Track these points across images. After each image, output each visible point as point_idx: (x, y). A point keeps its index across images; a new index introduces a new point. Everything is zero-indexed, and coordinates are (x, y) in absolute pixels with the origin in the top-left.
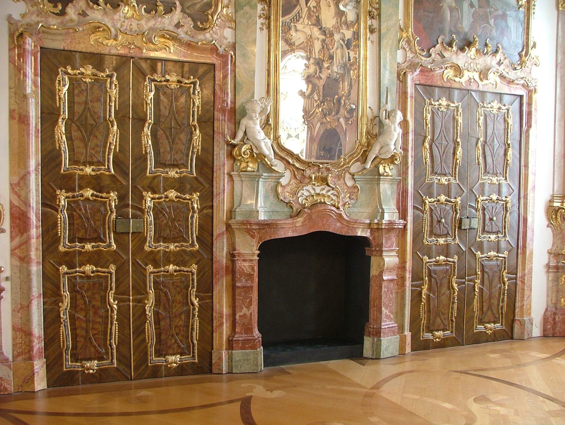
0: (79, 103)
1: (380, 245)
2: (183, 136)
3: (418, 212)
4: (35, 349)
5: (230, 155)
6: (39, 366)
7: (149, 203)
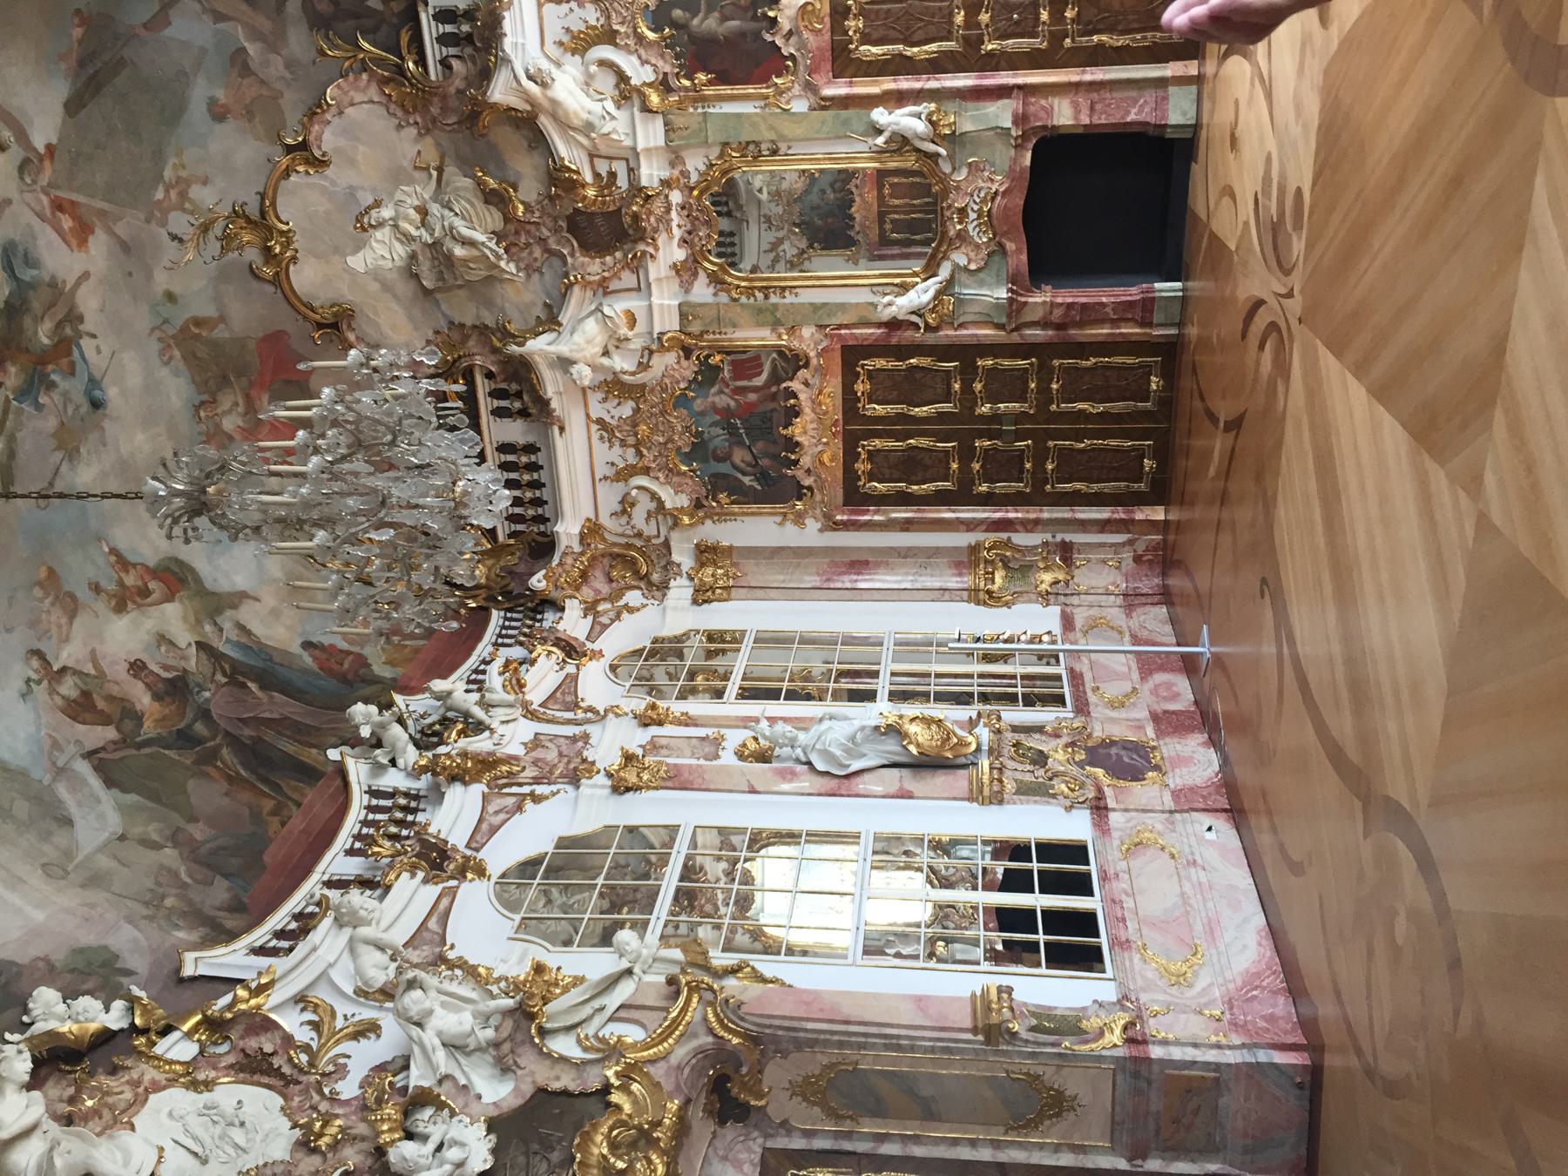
1: (1044, 127)
2: (918, 376)
3: (1003, 63)
4: (1123, 516)
5: (936, 329)
6: (1140, 514)
7: (986, 409)
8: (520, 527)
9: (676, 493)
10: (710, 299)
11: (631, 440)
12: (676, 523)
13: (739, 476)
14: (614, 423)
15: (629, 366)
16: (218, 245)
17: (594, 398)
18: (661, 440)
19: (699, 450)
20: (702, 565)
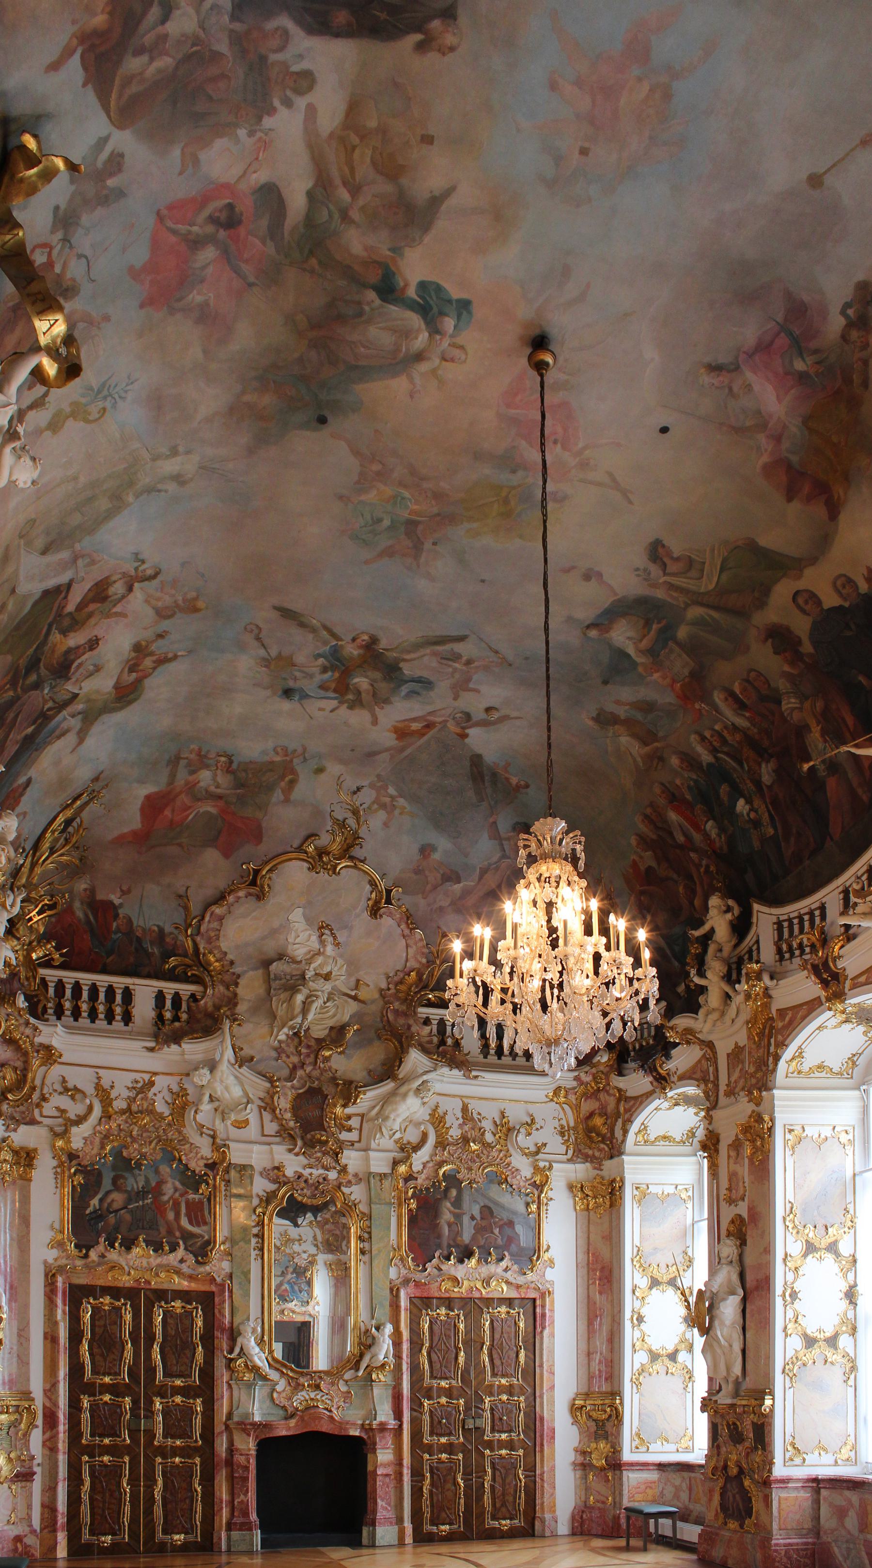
0: (100, 1326)
7: (158, 1405)
8: (51, 991)
9: (85, 1139)
10: (254, 1192)
11: (134, 1108)
12: (56, 1135)
13: (99, 1196)
14: (150, 1094)
15: (200, 1118)
16: (341, 818)
17: (173, 1082)
18: (135, 1133)
19: (124, 1164)
20: (16, 1152)
